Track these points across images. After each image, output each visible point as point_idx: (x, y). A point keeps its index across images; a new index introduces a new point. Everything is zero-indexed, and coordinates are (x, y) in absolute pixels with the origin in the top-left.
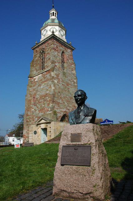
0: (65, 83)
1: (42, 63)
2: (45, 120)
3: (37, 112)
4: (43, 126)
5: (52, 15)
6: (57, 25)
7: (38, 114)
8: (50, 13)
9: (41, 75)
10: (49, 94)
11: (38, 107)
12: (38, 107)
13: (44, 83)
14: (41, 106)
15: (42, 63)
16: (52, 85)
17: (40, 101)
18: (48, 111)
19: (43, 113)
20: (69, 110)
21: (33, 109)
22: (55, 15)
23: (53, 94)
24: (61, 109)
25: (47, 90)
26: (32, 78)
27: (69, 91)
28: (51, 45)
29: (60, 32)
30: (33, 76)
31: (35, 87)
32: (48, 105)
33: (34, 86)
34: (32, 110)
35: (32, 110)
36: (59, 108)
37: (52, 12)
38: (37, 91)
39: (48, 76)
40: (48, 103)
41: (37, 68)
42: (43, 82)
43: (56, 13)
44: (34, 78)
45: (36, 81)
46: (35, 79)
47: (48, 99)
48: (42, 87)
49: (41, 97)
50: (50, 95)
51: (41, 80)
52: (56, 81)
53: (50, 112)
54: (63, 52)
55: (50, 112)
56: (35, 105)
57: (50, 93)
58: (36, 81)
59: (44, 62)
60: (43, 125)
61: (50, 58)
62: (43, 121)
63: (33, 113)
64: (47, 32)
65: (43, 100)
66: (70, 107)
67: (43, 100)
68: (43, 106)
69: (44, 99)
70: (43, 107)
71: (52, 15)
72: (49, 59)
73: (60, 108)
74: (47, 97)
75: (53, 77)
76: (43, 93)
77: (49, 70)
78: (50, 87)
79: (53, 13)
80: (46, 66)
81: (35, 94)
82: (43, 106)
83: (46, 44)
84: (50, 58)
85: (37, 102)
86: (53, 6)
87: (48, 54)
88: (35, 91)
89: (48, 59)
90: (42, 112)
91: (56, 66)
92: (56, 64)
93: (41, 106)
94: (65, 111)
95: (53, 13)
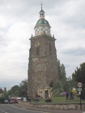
0: (51, 63)
3: (36, 80)
4: (46, 90)
7: (37, 82)
9: (37, 59)
10: (44, 71)
11: (36, 78)
12: (36, 78)
14: (39, 77)
16: (46, 67)
17: (38, 74)
18: (43, 80)
20: (53, 79)
21: (33, 78)
23: (46, 72)
27: (53, 68)
28: (44, 41)
29: (47, 30)
31: (33, 65)
32: (43, 77)
34: (32, 79)
35: (32, 79)
37: (41, 13)
39: (42, 60)
40: (43, 76)
42: (40, 63)
44: (33, 59)
45: (34, 61)
48: (39, 66)
49: (39, 72)
51: (38, 62)
52: (47, 64)
54: (50, 44)
58: (34, 61)
59: (39, 51)
60: (46, 89)
62: (46, 87)
65: (40, 74)
67: (40, 74)
68: (40, 77)
70: (40, 78)
72: (43, 50)
73: (50, 79)
74: (43, 73)
75: (46, 62)
76: (39, 70)
78: (44, 67)
79: (42, 14)
80: (41, 54)
82: (40, 77)
84: (43, 50)
85: (36, 74)
87: (42, 46)
88: (34, 68)
89: (42, 50)
90: (39, 81)
91: (47, 54)
92: (47, 53)
93: (39, 77)
94: (52, 80)
95: (42, 14)
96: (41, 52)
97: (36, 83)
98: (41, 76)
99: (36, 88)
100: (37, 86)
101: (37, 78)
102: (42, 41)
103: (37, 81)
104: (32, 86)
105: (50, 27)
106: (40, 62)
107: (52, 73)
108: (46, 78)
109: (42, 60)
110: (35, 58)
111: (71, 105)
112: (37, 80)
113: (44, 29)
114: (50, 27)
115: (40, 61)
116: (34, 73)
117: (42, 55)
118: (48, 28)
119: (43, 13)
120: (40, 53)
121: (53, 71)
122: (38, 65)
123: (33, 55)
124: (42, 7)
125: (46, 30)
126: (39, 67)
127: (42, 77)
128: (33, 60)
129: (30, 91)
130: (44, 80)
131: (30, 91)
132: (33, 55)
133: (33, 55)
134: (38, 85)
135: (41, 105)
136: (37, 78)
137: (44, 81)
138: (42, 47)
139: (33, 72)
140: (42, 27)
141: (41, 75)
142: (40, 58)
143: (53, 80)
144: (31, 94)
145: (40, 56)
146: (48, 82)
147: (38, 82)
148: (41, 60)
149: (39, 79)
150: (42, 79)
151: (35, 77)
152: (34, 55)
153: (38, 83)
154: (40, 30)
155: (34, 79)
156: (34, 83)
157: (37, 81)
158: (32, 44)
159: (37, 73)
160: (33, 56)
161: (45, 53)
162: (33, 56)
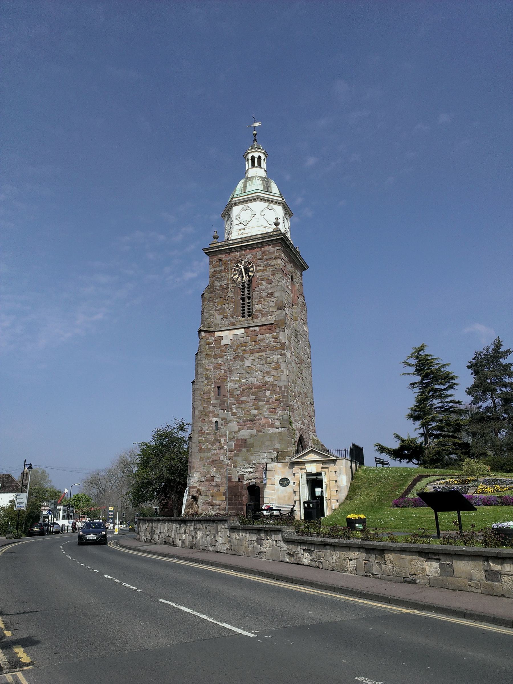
1: (243, 300)
3: (234, 426)
5: (256, 164)
6: (279, 203)
7: (235, 432)
8: (250, 156)
9: (242, 331)
10: (275, 386)
11: (234, 414)
12: (234, 414)
13: (257, 354)
15: (243, 300)
17: (243, 399)
18: (272, 426)
19: (254, 432)
21: (217, 416)
25: (268, 374)
26: (212, 334)
28: (276, 258)
30: (213, 329)
31: (220, 361)
32: (273, 410)
33: (216, 356)
34: (214, 420)
41: (230, 308)
42: (252, 352)
43: (263, 157)
44: (217, 334)
45: (223, 343)
46: (221, 338)
47: (273, 399)
48: (247, 364)
49: (247, 390)
50: (278, 388)
51: (244, 344)
56: (223, 406)
58: (223, 343)
60: (314, 465)
61: (272, 293)
63: (217, 429)
65: (252, 398)
67: (254, 397)
68: (255, 412)
69: (253, 394)
71: (256, 164)
74: (268, 393)
76: (254, 379)
77: (272, 324)
79: (259, 157)
80: (260, 311)
81: (223, 379)
82: (255, 412)
83: (258, 253)
84: (272, 293)
86: (255, 135)
89: (265, 294)
90: (249, 428)
96: (260, 303)
97: (231, 440)
100: (240, 451)
101: (240, 414)
102: (265, 257)
103: (236, 428)
109: (268, 335)
110: (233, 327)
117: (265, 315)
120: (257, 307)
122: (242, 360)
123: (219, 317)
126: (248, 370)
127: (266, 413)
128: (221, 338)
129: (203, 478)
131: (203, 478)
132: (220, 314)
133: (219, 317)
134: (244, 450)
137: (272, 430)
138: (264, 283)
139: (219, 387)
142: (257, 329)
147: (245, 433)
148: (259, 337)
149: (250, 421)
151: (231, 409)
153: (245, 440)
156: (222, 440)
157: (240, 429)
158: (217, 269)
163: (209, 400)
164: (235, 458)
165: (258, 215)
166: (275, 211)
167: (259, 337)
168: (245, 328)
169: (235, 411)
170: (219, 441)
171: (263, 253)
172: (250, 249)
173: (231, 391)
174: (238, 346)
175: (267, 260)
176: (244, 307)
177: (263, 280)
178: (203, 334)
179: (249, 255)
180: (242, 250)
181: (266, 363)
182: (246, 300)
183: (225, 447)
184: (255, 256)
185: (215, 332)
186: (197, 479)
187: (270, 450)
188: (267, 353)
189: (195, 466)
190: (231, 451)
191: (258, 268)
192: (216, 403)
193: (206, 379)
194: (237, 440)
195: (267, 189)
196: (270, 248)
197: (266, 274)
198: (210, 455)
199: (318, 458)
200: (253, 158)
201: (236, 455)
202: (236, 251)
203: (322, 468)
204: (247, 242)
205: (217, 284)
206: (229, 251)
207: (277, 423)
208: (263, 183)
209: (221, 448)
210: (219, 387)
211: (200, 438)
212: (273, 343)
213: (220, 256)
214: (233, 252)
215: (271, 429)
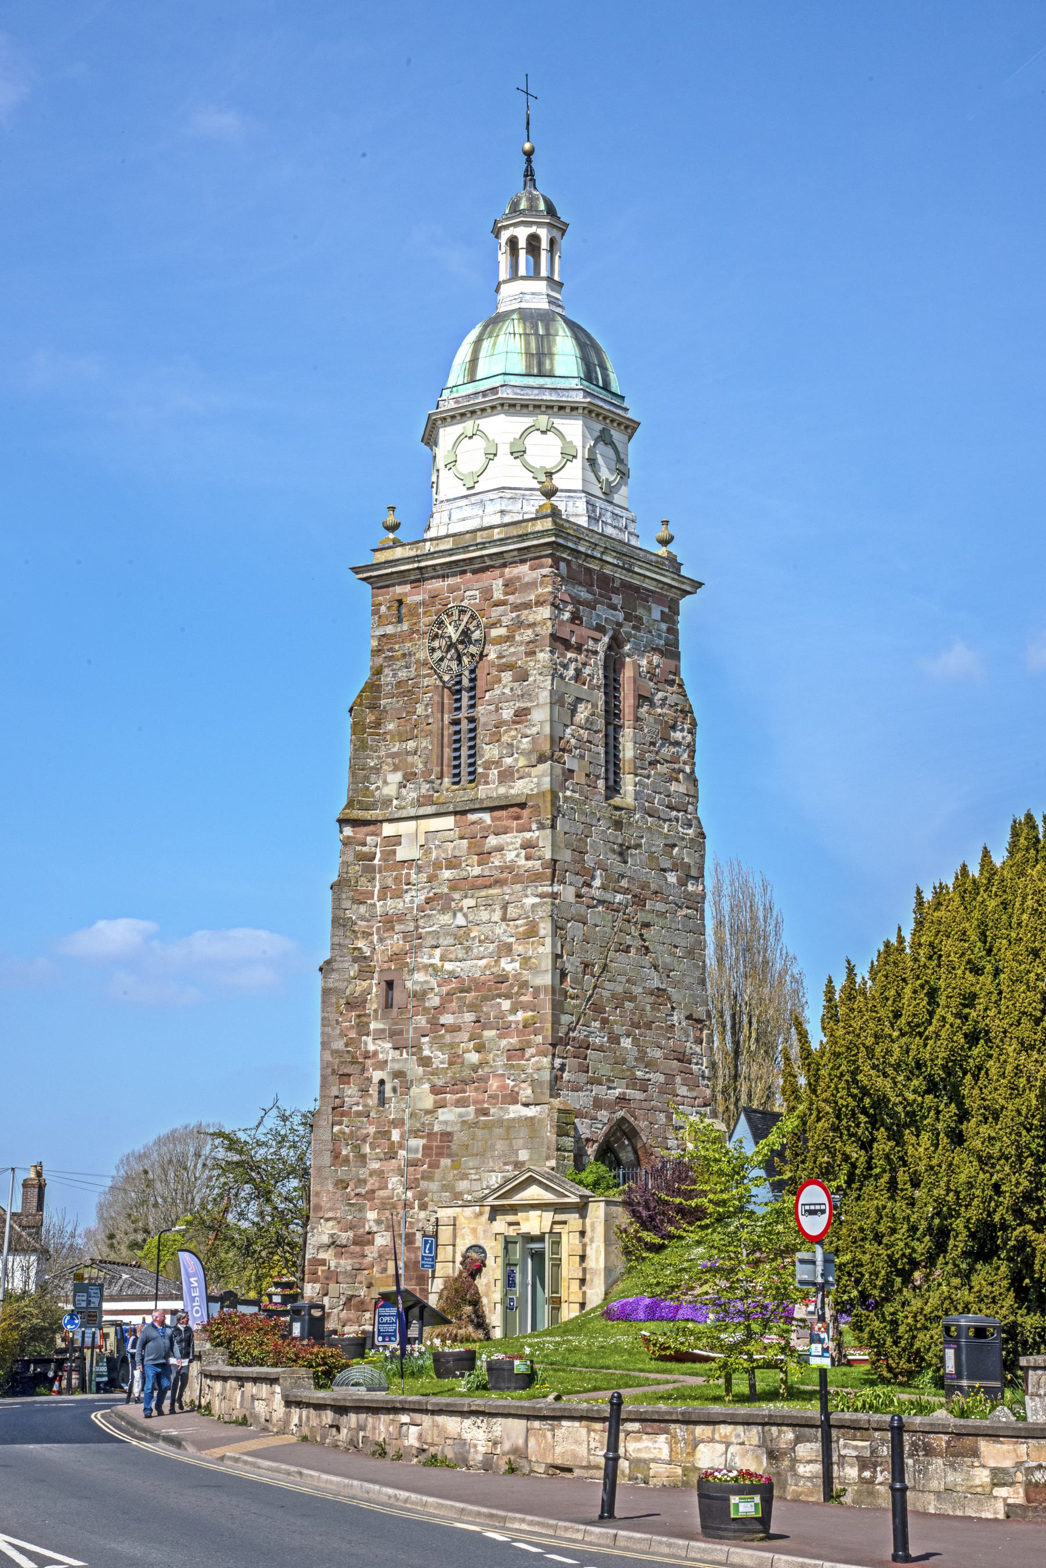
1: (456, 722)
2: (547, 1188)
3: (423, 1096)
7: (428, 1112)
8: (505, 235)
9: (449, 822)
10: (524, 985)
11: (425, 1062)
12: (425, 1062)
14: (455, 1059)
16: (545, 928)
17: (447, 1019)
21: (382, 1065)
22: (544, 272)
24: (596, 1089)
25: (507, 949)
26: (371, 828)
34: (377, 1075)
36: (583, 1078)
37: (522, 234)
38: (415, 938)
44: (388, 829)
45: (403, 853)
52: (568, 893)
53: (531, 1112)
55: (531, 1112)
57: (526, 975)
58: (403, 853)
60: (534, 1214)
62: (534, 1193)
63: (382, 1101)
64: (491, 455)
65: (469, 1017)
66: (650, 1065)
67: (469, 1017)
68: (474, 1057)
69: (473, 1007)
70: (475, 1068)
71: (522, 272)
73: (592, 1082)
77: (522, 806)
78: (532, 932)
79: (533, 241)
82: (474, 1057)
85: (422, 1021)
86: (529, 154)
89: (507, 714)
90: (461, 1103)
93: (455, 1059)
94: (622, 1099)
97: (416, 1133)
98: (478, 1049)
99: (421, 1196)
101: (440, 1058)
102: (511, 598)
103: (429, 1102)
104: (375, 1165)
105: (630, 427)
106: (477, 871)
107: (629, 1005)
108: (546, 1076)
111: (725, 1430)
112: (435, 1090)
113: (544, 451)
114: (630, 427)
115: (484, 856)
116: (398, 996)
118: (604, 438)
119: (543, 233)
121: (637, 990)
124: (529, 154)
125: (568, 456)
128: (396, 840)
129: (345, 1237)
130: (526, 1092)
132: (396, 769)
133: (396, 778)
134: (445, 1162)
135: (405, 1418)
136: (440, 1058)
137: (516, 1111)
138: (507, 677)
139: (390, 985)
140: (526, 421)
141: (489, 1034)
142: (486, 817)
143: (638, 1095)
144: (346, 1264)
145: (482, 791)
146: (565, 1122)
148: (492, 841)
149: (456, 1084)
150: (494, 1084)
152: (409, 777)
153: (447, 1136)
154: (491, 455)
155: (399, 1074)
156: (396, 1135)
158: (390, 629)
159: (436, 1001)
160: (390, 790)
161: (554, 750)
162: (390, 783)
163: (365, 1019)
164: (424, 1184)
165: (504, 456)
166: (560, 435)
167: (492, 841)
168: (455, 813)
169: (426, 1053)
170: (387, 1134)
171: (506, 585)
172: (475, 572)
173: (420, 996)
174: (437, 866)
175: (516, 608)
176: (458, 749)
177: (503, 668)
178: (348, 831)
179: (469, 591)
180: (454, 575)
181: (504, 919)
182: (465, 726)
183: (402, 1153)
184: (487, 593)
185: (381, 821)
186: (325, 1239)
187: (505, 1164)
188: (507, 889)
189: (323, 1204)
190: (413, 1163)
191: (495, 633)
192: (383, 1031)
193: (355, 960)
194: (431, 1135)
195: (539, 360)
196: (523, 570)
197: (512, 650)
198: (363, 1173)
199: (548, 1197)
200: (513, 242)
201: (428, 1177)
202: (438, 577)
203: (554, 1223)
204: (464, 553)
205: (387, 678)
206: (420, 576)
207: (526, 1092)
208: (528, 344)
209: (391, 1155)
210: (390, 985)
211: (336, 1128)
212: (522, 862)
213: (399, 590)
214: (432, 578)
215: (512, 1108)
